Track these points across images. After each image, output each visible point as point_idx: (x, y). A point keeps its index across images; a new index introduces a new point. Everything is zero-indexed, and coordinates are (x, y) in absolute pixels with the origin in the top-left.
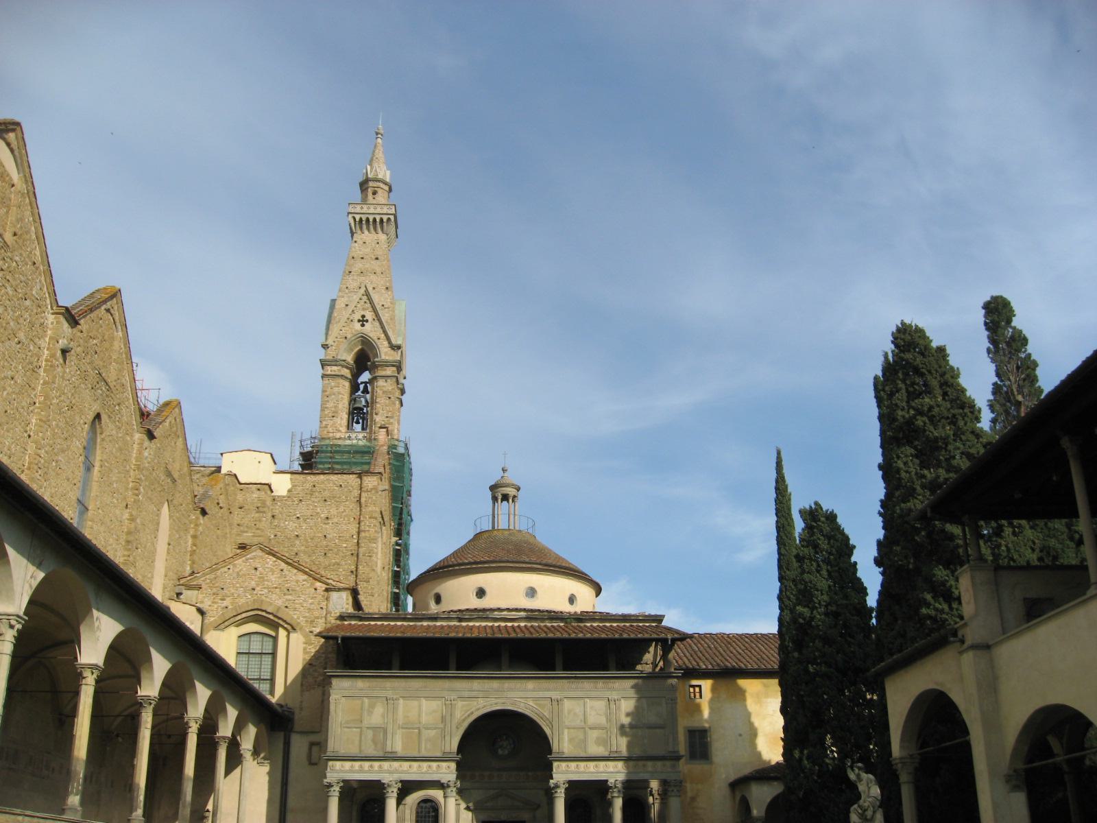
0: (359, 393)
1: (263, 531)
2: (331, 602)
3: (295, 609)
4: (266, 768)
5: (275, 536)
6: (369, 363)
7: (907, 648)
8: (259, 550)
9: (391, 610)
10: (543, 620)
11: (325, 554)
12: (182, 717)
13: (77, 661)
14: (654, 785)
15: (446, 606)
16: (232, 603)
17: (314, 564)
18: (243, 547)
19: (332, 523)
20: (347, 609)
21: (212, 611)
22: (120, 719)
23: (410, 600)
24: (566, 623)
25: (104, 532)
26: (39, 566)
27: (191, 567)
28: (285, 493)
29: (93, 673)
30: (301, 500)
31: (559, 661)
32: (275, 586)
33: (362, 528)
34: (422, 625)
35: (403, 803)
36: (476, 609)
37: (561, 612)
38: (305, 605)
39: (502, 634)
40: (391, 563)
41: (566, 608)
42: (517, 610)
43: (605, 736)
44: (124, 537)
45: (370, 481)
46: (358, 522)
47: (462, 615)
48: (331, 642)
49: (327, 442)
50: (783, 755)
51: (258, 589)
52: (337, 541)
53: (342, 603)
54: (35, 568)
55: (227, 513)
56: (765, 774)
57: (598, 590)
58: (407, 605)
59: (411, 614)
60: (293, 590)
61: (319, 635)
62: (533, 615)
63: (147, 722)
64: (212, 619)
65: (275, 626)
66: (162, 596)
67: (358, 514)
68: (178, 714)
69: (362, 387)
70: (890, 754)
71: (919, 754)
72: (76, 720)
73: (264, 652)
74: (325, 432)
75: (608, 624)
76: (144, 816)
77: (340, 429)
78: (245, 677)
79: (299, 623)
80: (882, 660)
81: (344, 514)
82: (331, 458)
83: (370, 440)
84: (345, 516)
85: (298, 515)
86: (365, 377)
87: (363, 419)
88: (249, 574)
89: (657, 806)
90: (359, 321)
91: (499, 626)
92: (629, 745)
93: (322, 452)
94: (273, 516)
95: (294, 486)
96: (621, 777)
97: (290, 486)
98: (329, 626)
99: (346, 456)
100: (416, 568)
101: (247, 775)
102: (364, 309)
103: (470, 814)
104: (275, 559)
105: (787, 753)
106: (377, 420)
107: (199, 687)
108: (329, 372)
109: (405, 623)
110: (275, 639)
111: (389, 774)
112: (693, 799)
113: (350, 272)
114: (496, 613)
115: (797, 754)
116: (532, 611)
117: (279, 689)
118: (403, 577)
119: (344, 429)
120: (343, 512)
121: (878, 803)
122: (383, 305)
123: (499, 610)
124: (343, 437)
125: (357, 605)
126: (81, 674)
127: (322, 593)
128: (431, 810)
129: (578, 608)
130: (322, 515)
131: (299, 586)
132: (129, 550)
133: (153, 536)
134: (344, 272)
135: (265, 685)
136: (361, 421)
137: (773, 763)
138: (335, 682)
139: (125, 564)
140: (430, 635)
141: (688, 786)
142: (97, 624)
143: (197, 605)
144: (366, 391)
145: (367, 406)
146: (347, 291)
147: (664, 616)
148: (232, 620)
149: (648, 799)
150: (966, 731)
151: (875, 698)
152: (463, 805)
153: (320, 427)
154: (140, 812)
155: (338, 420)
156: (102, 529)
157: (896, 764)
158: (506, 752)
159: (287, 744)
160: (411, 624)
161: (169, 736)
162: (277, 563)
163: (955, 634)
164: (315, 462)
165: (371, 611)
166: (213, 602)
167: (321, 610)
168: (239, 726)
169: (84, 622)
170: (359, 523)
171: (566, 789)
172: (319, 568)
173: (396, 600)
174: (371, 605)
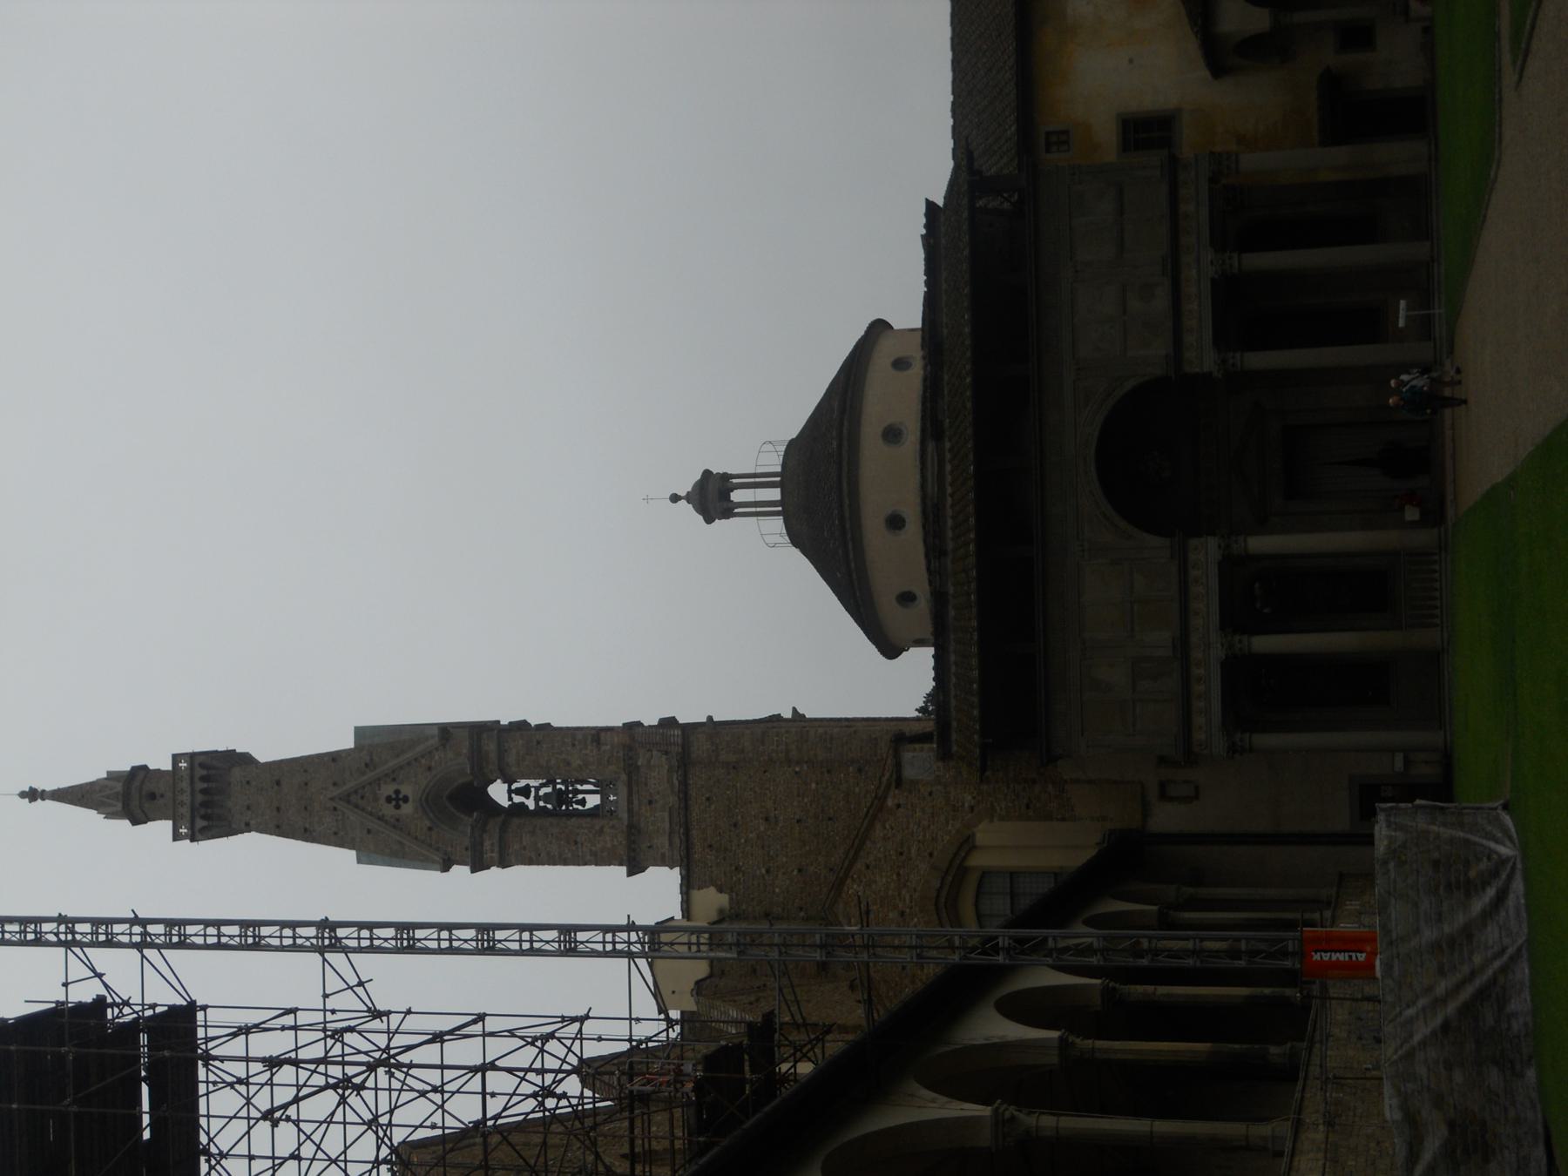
0: (531, 804)
5: (801, 909)
6: (475, 784)
11: (830, 819)
19: (775, 810)
28: (723, 900)
30: (736, 869)
32: (895, 877)
36: (924, 527)
41: (917, 372)
52: (806, 800)
53: (919, 763)
69: (517, 799)
73: (1008, 891)
77: (597, 828)
81: (757, 789)
85: (763, 871)
86: (498, 792)
87: (578, 792)
90: (398, 807)
95: (713, 883)
97: (712, 890)
102: (376, 799)
104: (849, 881)
106: (579, 762)
108: (495, 855)
110: (985, 874)
113: (306, 830)
116: (923, 431)
120: (755, 792)
122: (367, 765)
130: (762, 828)
134: (306, 840)
136: (580, 797)
144: (525, 792)
145: (551, 782)
146: (342, 833)
162: (855, 876)
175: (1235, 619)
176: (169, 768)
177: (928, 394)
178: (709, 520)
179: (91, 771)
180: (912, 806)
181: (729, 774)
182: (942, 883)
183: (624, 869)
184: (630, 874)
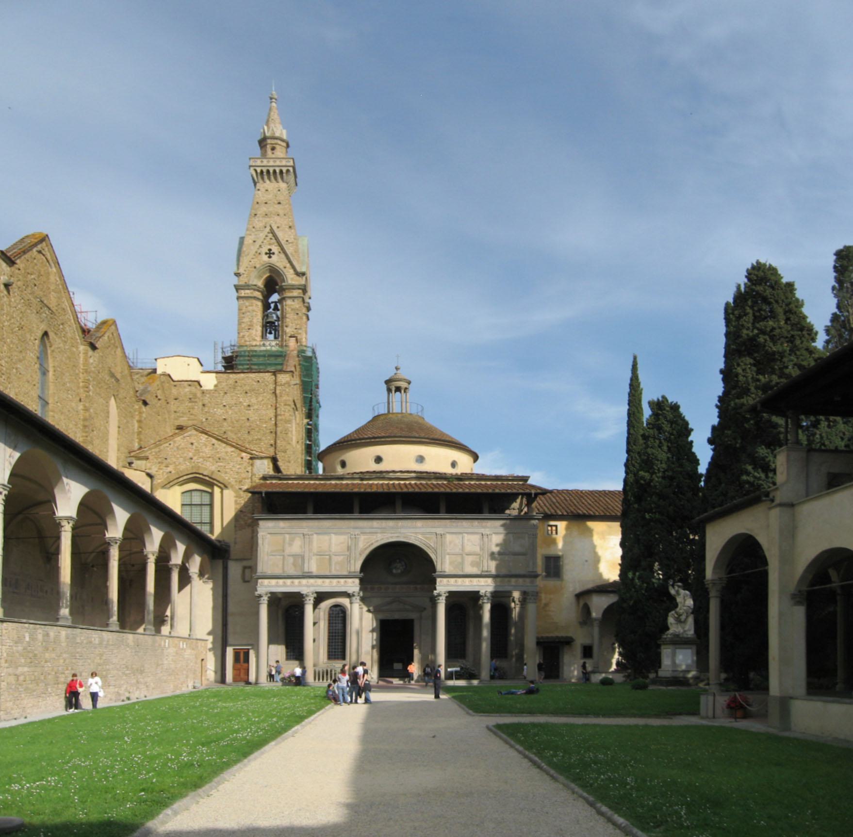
1: (195, 416)
2: (255, 467)
3: (226, 473)
4: (210, 585)
7: (727, 504)
8: (194, 430)
9: (305, 472)
10: (430, 479)
12: (142, 552)
13: (55, 515)
14: (516, 595)
15: (350, 469)
16: (175, 469)
17: (240, 440)
18: (180, 428)
19: (254, 410)
20: (269, 472)
21: (159, 475)
22: (93, 555)
23: (320, 465)
24: (449, 481)
25: (65, 419)
26: (15, 448)
27: (139, 443)
28: (212, 387)
29: (69, 523)
30: (226, 393)
32: (208, 456)
33: (279, 412)
34: (331, 484)
35: (318, 607)
37: (445, 474)
38: (234, 469)
39: (396, 489)
40: (304, 438)
41: (449, 470)
42: (408, 472)
43: (478, 560)
44: (82, 423)
45: (283, 378)
46: (274, 408)
47: (363, 476)
48: (257, 496)
49: (245, 348)
50: (620, 576)
51: (195, 458)
53: (264, 467)
54: (11, 450)
55: (165, 403)
56: (604, 589)
57: (476, 457)
58: (318, 469)
59: (321, 475)
60: (223, 459)
61: (247, 491)
62: (421, 475)
63: (114, 556)
64: (159, 481)
65: (211, 485)
66: (117, 465)
67: (275, 402)
68: (138, 550)
70: (704, 577)
71: (727, 578)
72: (60, 556)
74: (243, 341)
75: (483, 483)
76: (119, 620)
78: (190, 522)
79: (230, 483)
80: (706, 511)
81: (263, 402)
82: (249, 360)
83: (282, 346)
84: (264, 404)
85: (225, 404)
87: (275, 330)
88: (187, 448)
89: (517, 609)
91: (393, 484)
92: (497, 567)
93: (241, 356)
94: (204, 405)
96: (490, 589)
98: (254, 484)
99: (261, 359)
100: (324, 442)
101: (195, 590)
103: (370, 615)
105: (623, 574)
107: (154, 529)
109: (317, 482)
112: (546, 605)
114: (391, 474)
115: (630, 575)
117: (217, 530)
118: (314, 448)
119: (259, 338)
121: (691, 611)
123: (394, 472)
124: (258, 344)
125: (277, 469)
126: (59, 523)
127: (248, 461)
128: (340, 612)
129: (458, 471)
130: (245, 404)
131: (228, 456)
132: (86, 432)
133: (105, 421)
135: (206, 527)
136: (273, 332)
137: (611, 581)
138: (261, 523)
139: (83, 442)
140: (338, 490)
141: (543, 596)
142: (67, 488)
143: (147, 471)
147: (529, 477)
148: (176, 481)
149: (510, 604)
150: (764, 561)
151: (697, 538)
152: (365, 609)
153: (238, 337)
154: (115, 618)
155: (253, 332)
156: (62, 417)
157: (708, 584)
160: (322, 482)
161: (133, 565)
163: (767, 495)
164: (236, 364)
165: (289, 473)
166: (159, 469)
167: (247, 473)
168: (187, 556)
169: (57, 487)
170: (276, 409)
171: (447, 597)
172: (244, 443)
173: (309, 465)
174: (288, 469)
177: (438, 475)
180: (242, 464)
181: (271, 390)
182: (205, 476)
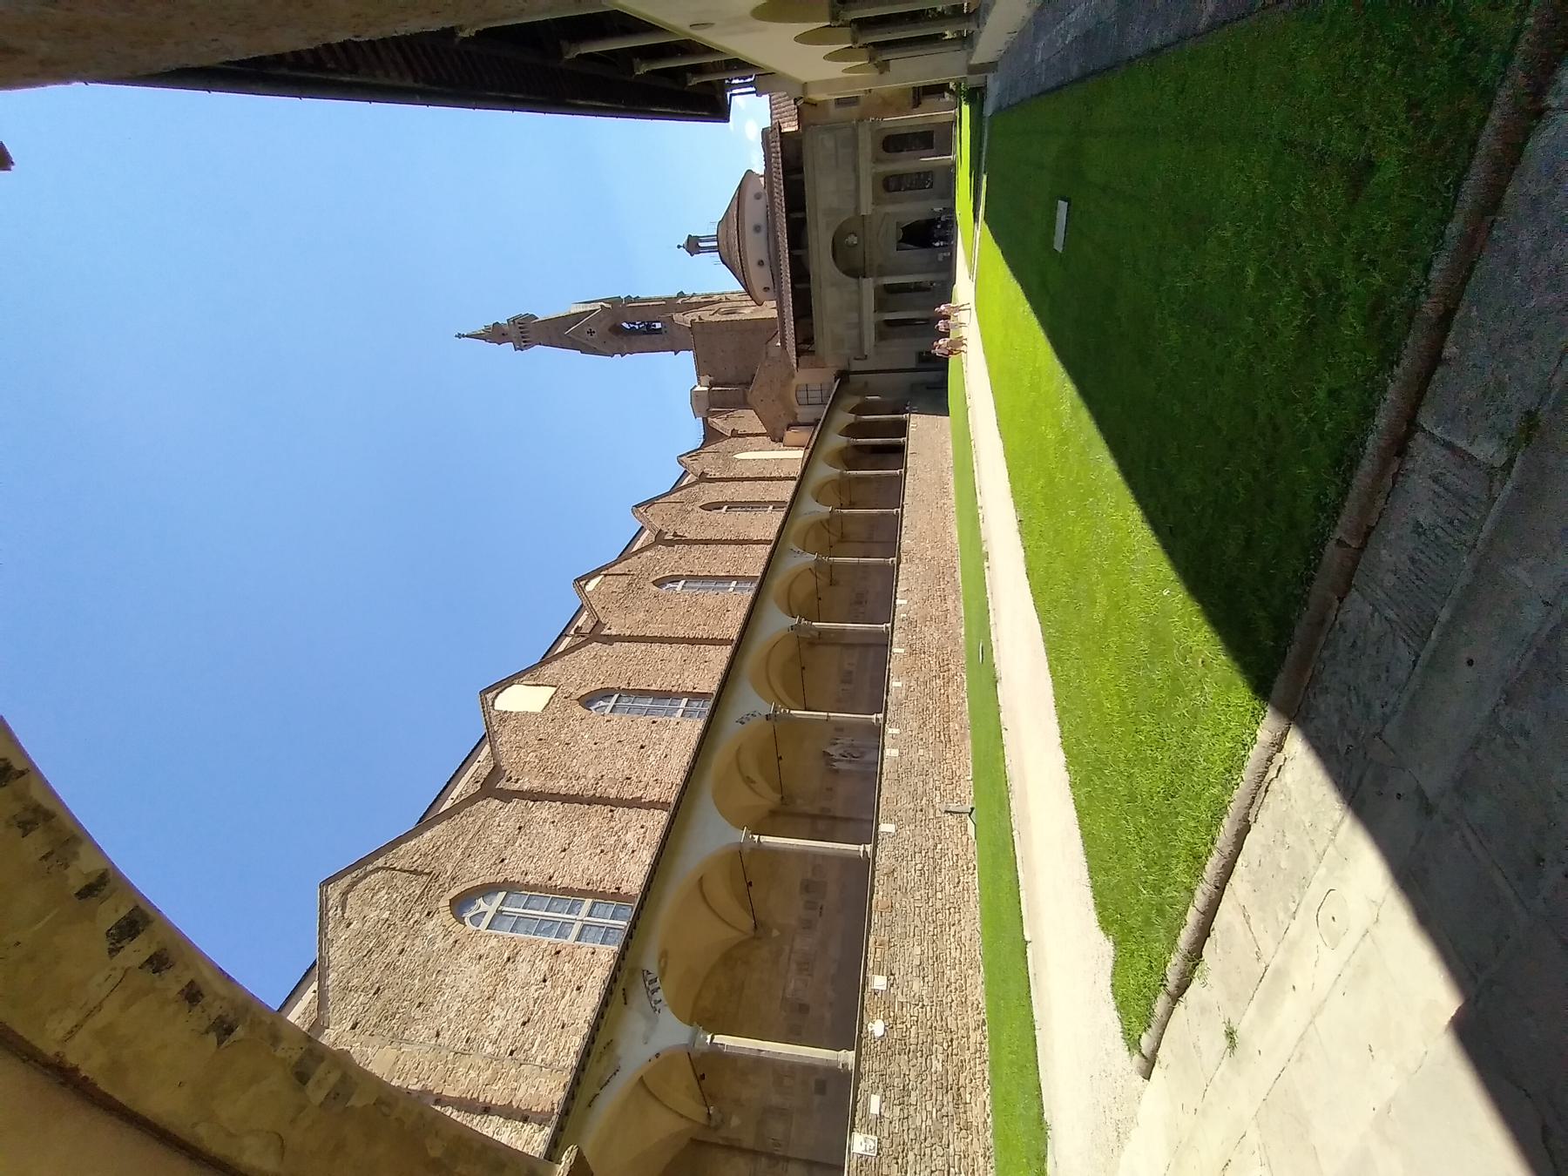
0: (637, 327)
28: (712, 378)
31: (799, 215)
69: (632, 326)
86: (625, 324)
111: (870, 317)
144: (634, 324)
158: (856, 238)
159: (856, 373)
175: (880, 306)
176: (506, 322)
178: (692, 255)
179: (479, 328)
183: (673, 353)
184: (676, 354)
